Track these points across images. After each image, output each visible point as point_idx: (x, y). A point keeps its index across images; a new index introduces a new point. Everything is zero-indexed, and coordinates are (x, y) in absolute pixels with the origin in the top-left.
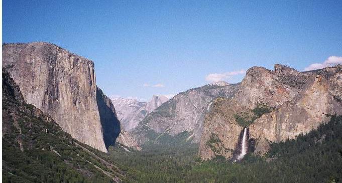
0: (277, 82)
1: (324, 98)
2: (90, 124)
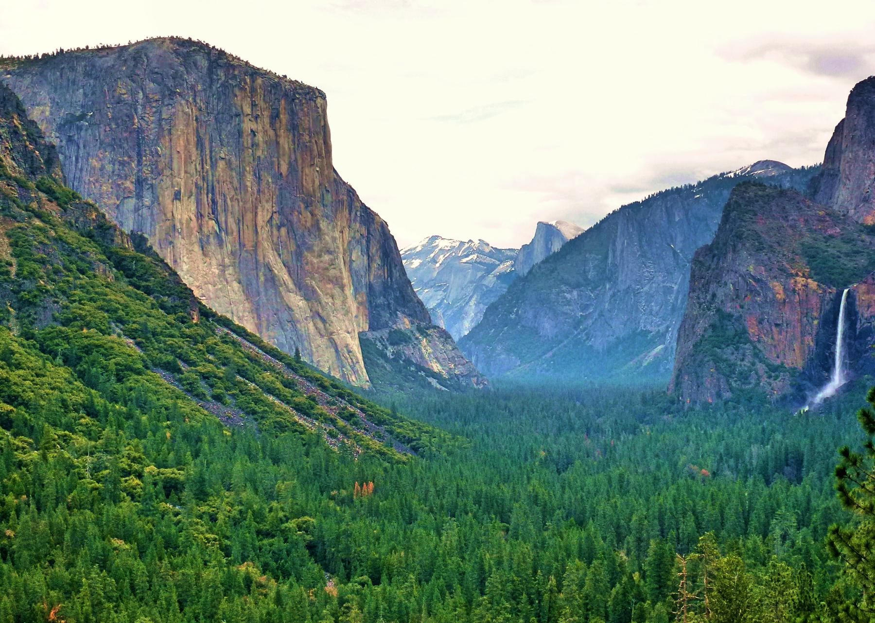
2: (309, 295)
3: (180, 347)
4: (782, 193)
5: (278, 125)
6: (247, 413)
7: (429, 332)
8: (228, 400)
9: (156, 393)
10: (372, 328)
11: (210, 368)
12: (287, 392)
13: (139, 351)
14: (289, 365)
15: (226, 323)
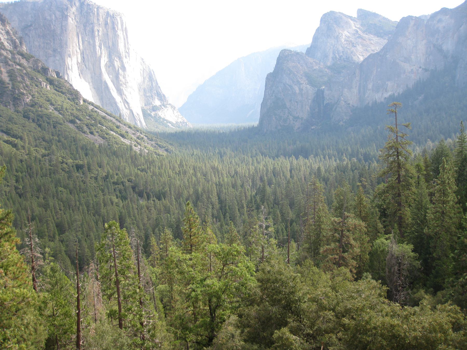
0: (360, 32)
1: (422, 47)
3: (76, 114)
4: (297, 53)
5: (107, 28)
6: (103, 139)
7: (167, 106)
8: (95, 133)
9: (69, 132)
10: (145, 105)
11: (89, 121)
12: (118, 130)
13: (61, 116)
14: (117, 120)
15: (92, 104)
